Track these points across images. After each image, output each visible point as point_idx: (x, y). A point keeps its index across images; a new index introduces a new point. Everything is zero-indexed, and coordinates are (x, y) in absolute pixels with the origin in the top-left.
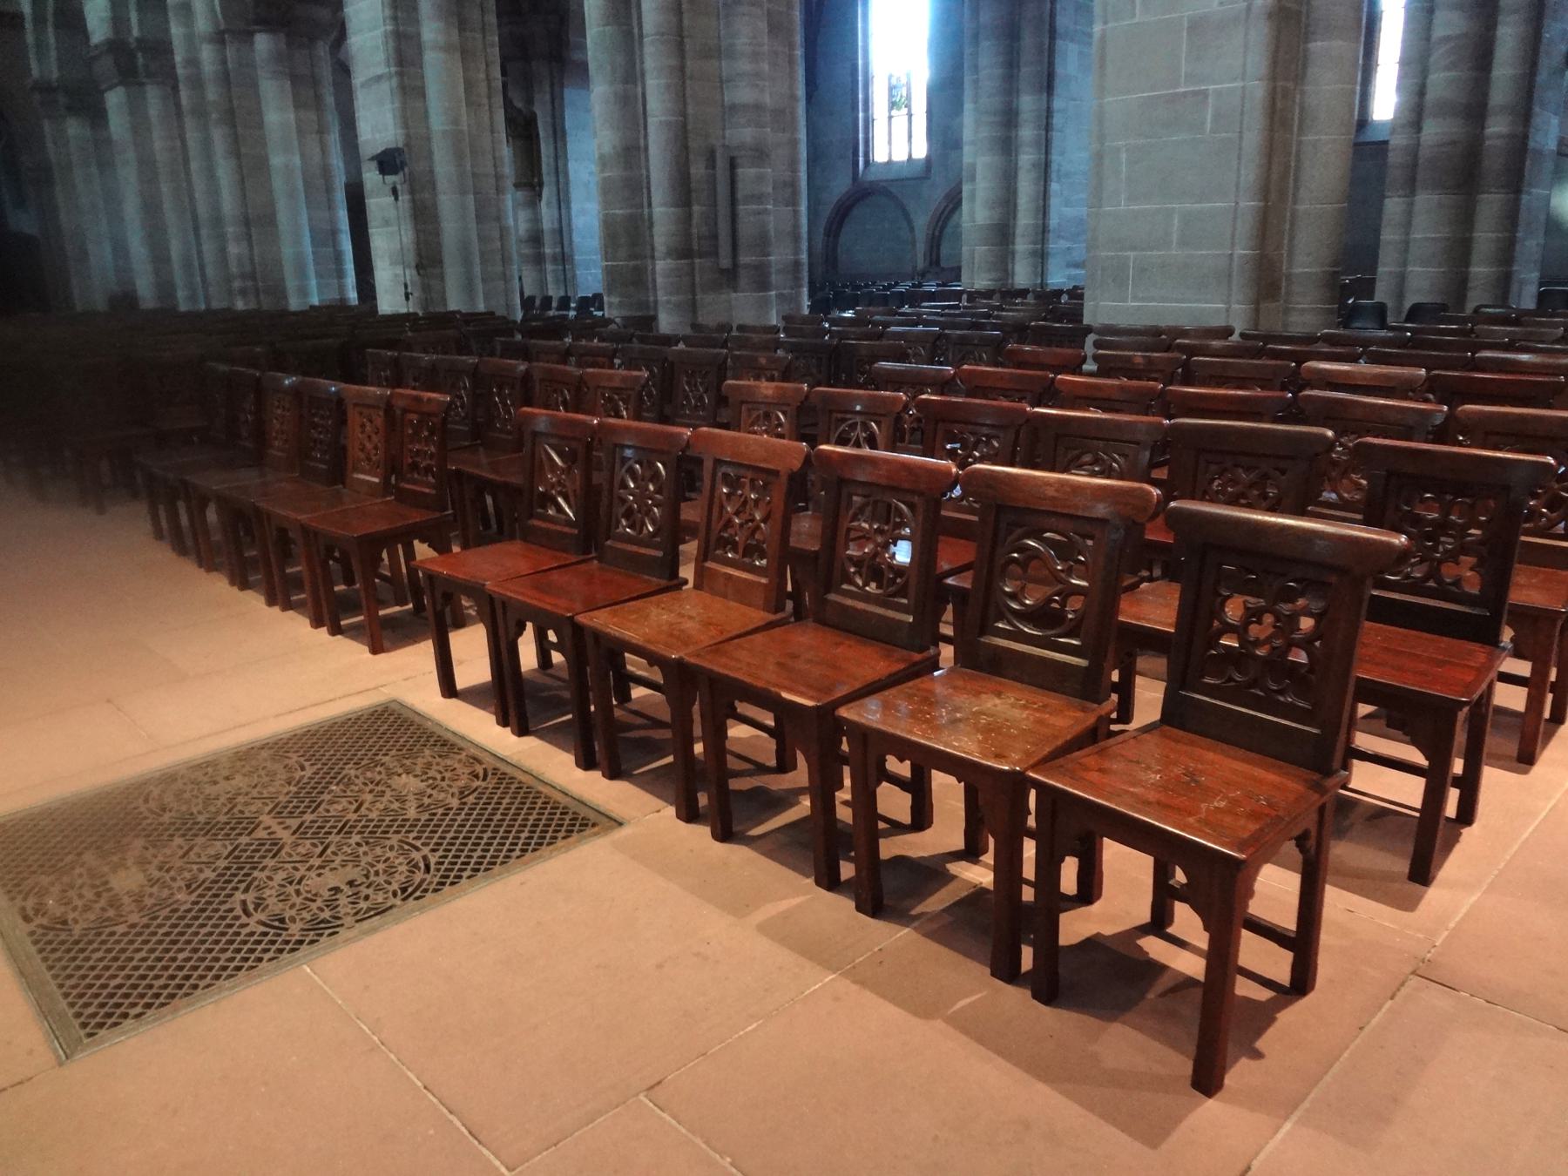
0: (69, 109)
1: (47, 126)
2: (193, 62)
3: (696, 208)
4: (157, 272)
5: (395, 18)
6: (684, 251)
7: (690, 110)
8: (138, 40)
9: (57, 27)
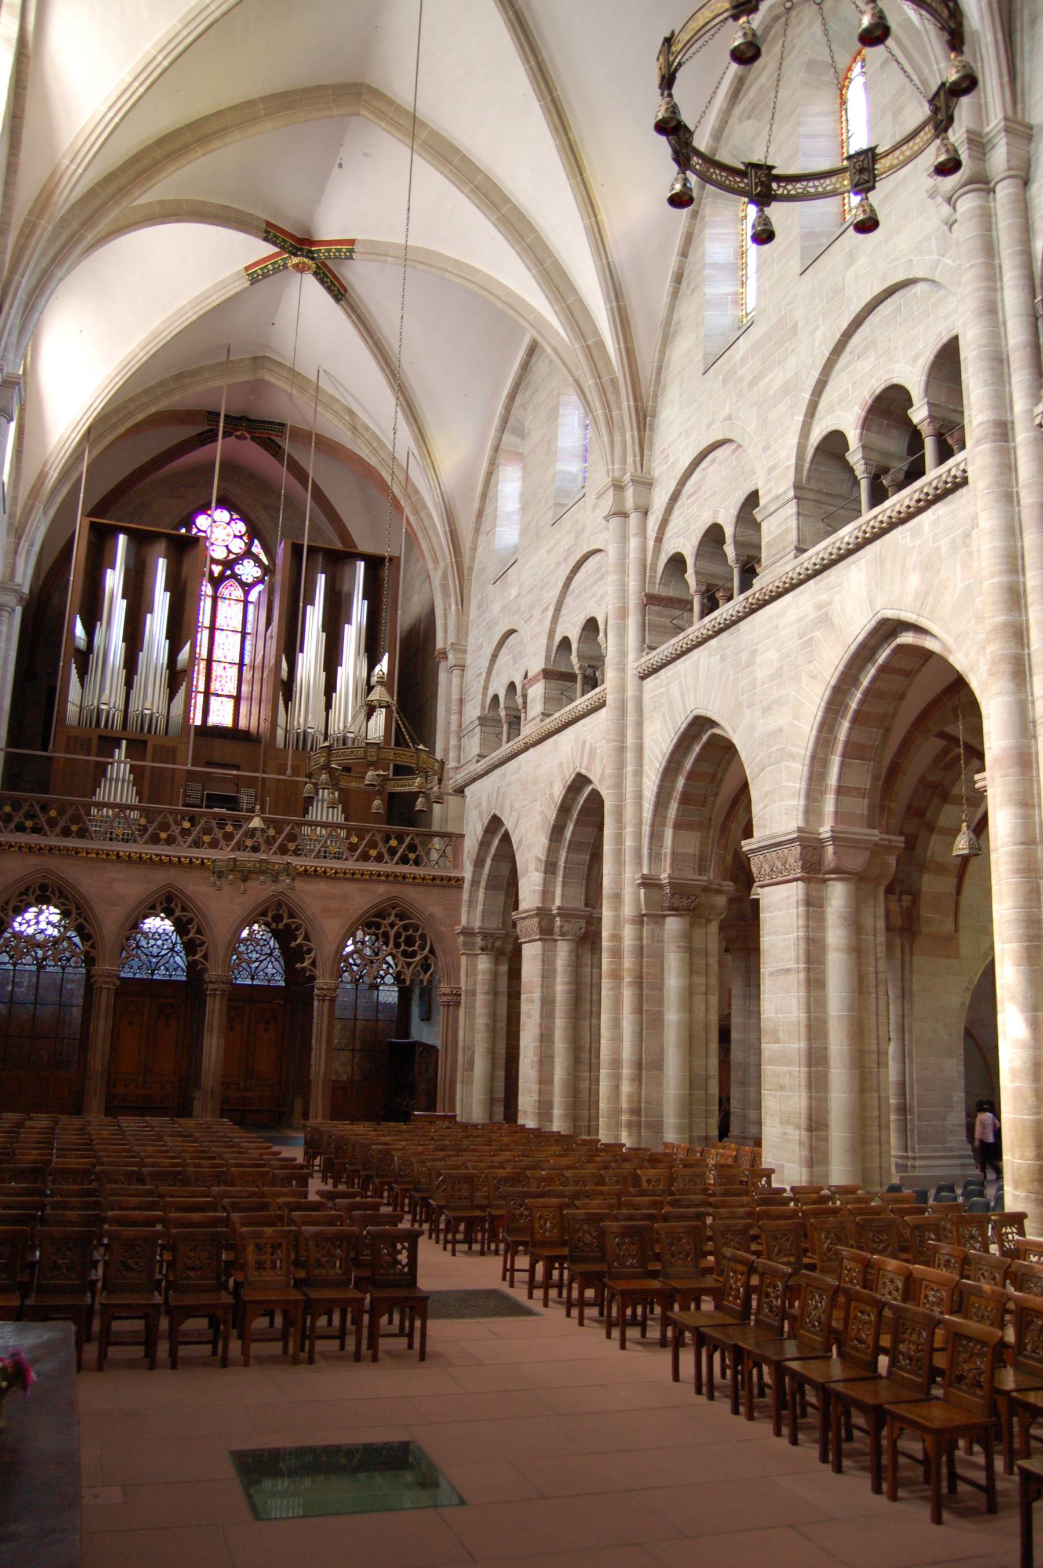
0: (483, 949)
1: (464, 959)
2: (617, 937)
5: (807, 927)
8: (559, 908)
9: (486, 889)
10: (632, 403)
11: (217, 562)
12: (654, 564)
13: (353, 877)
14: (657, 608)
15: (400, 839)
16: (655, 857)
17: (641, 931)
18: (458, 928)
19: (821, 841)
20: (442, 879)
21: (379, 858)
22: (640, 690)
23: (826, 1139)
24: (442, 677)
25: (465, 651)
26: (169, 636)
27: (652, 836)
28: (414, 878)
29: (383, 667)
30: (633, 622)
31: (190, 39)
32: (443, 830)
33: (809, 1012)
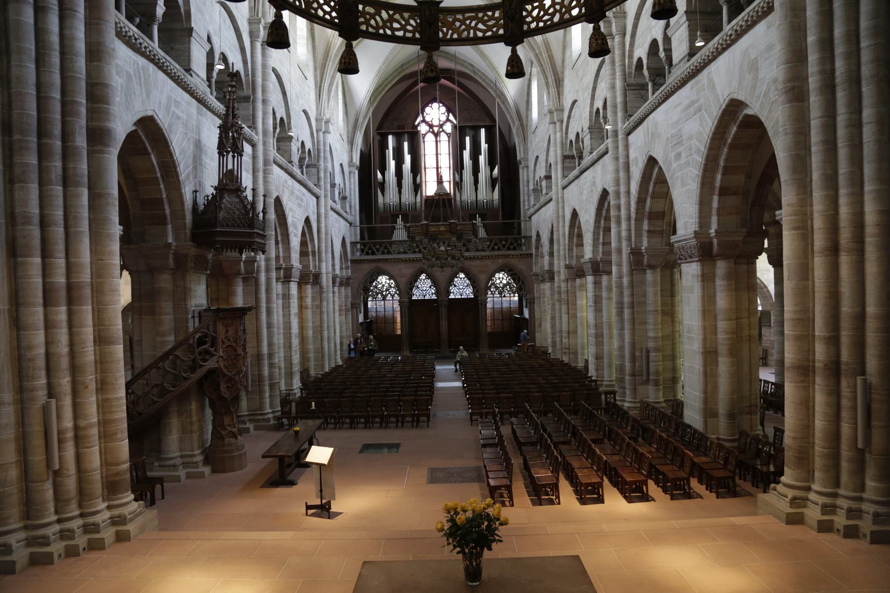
1: (535, 285)
2: (559, 287)
3: (637, 364)
4: (553, 338)
5: (595, 291)
6: (633, 375)
10: (553, 78)
11: (436, 126)
12: (566, 143)
13: (489, 257)
14: (568, 160)
15: (506, 241)
16: (571, 257)
20: (524, 255)
21: (499, 249)
22: (563, 193)
23: (603, 362)
24: (521, 171)
25: (528, 160)
26: (412, 172)
27: (569, 250)
28: (513, 256)
29: (496, 171)
30: (559, 166)
33: (596, 320)
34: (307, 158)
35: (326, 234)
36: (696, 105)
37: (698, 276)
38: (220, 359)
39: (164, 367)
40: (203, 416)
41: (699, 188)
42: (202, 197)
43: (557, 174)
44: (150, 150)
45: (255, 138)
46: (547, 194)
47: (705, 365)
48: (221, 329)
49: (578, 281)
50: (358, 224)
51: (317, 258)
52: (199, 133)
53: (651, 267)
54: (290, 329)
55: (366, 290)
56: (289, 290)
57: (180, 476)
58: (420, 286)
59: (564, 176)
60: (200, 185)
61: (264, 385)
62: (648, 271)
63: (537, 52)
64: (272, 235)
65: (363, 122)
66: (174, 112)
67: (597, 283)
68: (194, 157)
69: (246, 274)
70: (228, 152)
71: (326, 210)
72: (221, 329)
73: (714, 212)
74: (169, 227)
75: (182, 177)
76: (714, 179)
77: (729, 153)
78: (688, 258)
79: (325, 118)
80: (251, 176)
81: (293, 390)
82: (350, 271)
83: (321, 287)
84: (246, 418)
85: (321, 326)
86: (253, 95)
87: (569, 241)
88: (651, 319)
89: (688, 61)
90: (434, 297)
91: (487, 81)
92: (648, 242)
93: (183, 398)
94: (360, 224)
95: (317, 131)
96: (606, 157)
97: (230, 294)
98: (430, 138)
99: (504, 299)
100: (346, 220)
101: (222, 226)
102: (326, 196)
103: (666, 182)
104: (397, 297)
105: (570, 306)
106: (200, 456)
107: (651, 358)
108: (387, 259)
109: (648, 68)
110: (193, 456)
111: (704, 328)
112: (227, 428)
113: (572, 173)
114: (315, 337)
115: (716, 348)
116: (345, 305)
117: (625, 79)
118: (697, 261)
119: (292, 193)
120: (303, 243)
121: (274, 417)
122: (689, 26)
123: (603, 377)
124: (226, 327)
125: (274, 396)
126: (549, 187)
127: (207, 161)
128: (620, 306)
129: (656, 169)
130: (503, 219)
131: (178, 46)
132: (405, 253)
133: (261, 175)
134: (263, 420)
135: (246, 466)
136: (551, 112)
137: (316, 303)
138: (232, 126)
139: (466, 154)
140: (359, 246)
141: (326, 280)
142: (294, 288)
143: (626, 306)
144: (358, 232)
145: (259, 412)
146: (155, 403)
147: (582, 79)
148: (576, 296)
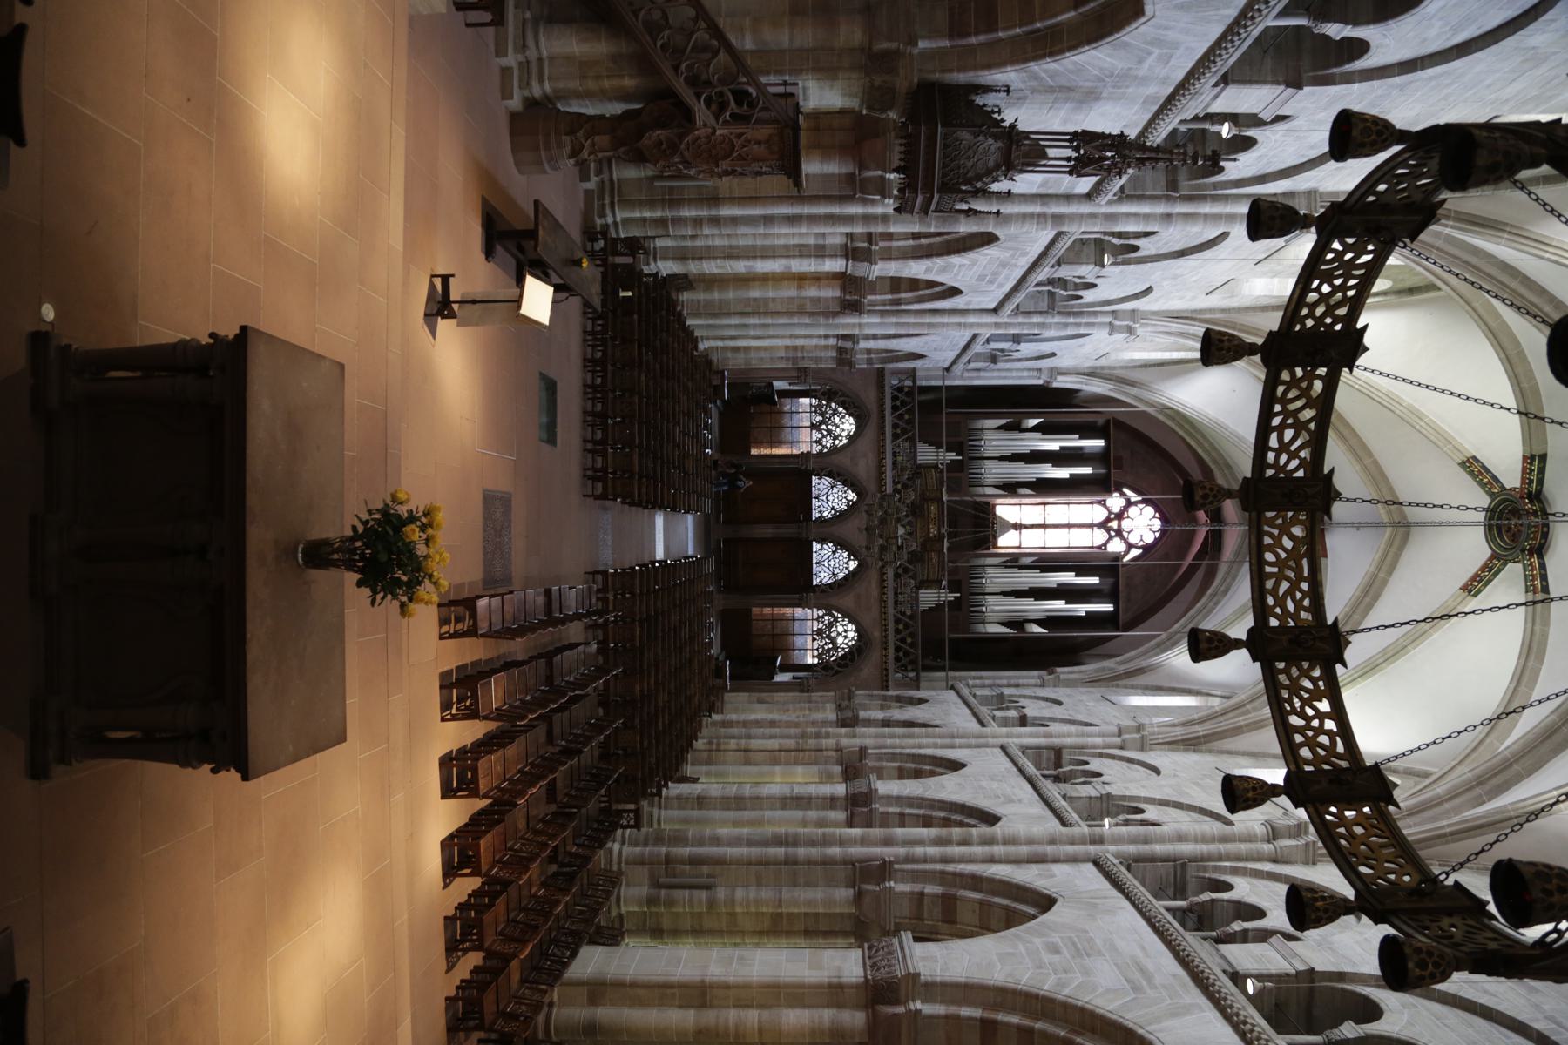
1: (832, 694)
2: (828, 736)
3: (688, 867)
4: (738, 722)
5: (818, 798)
6: (668, 860)
7: (734, 867)
11: (1119, 525)
12: (1084, 754)
14: (1053, 757)
15: (912, 645)
16: (880, 757)
17: (831, 750)
18: (853, 689)
19: (871, 805)
20: (887, 675)
21: (897, 631)
22: (993, 746)
23: (693, 809)
24: (1035, 673)
25: (1055, 686)
27: (893, 754)
28: (886, 656)
30: (1042, 741)
31: (1376, 398)
32: (922, 679)
33: (767, 798)
34: (1066, 293)
35: (930, 325)
36: (1144, 983)
37: (839, 977)
38: (710, 130)
39: (699, 30)
40: (610, 99)
41: (997, 983)
42: (998, 102)
43: (1028, 737)
44: (1082, 10)
45: (1103, 200)
46: (994, 718)
47: (683, 986)
48: (764, 132)
49: (838, 769)
50: (948, 383)
51: (888, 308)
52: (1112, 98)
53: (859, 897)
54: (763, 257)
55: (829, 395)
56: (831, 256)
57: (506, 55)
58: (835, 490)
59: (1024, 749)
60: (1019, 99)
61: (663, 209)
62: (850, 892)
63: (1248, 707)
64: (930, 227)
65: (1128, 395)
66: (1150, 54)
67: (831, 802)
68: (1069, 89)
69: (860, 180)
70: (1076, 149)
71: (972, 325)
72: (764, 132)
73: (953, 1010)
74: (945, 43)
75: (1034, 66)
76: (1012, 1010)
77: (1058, 1038)
78: (871, 962)
79: (1137, 325)
80: (1034, 191)
81: (655, 261)
82: (865, 366)
83: (835, 314)
84: (606, 176)
85: (766, 314)
86: (1179, 197)
87: (908, 755)
88: (766, 894)
89: (1224, 972)
90: (815, 515)
91: (1198, 617)
92: (903, 893)
93: (643, 63)
94: (947, 387)
95: (1113, 311)
96: (1056, 823)
97: (826, 151)
98: (1099, 514)
99: (809, 639)
100: (954, 362)
101: (946, 137)
102: (997, 325)
103: (1008, 928)
104: (816, 449)
105: (793, 753)
106: (541, 92)
107: (696, 893)
108: (883, 433)
109: (1213, 901)
110: (541, 80)
111: (746, 986)
112: (589, 141)
113: (1029, 763)
114: (748, 301)
115: (711, 1007)
116: (803, 358)
117: (1194, 859)
118: (866, 977)
119: (1004, 265)
120: (914, 284)
121: (607, 225)
122: (1287, 975)
123: (666, 808)
124: (767, 141)
125: (644, 226)
126: (1005, 722)
127: (1063, 113)
128: (790, 840)
129: (1032, 911)
130: (950, 640)
131: (1269, 63)
132: (894, 464)
133: (1037, 208)
134: (603, 205)
135: (521, 172)
136: (1140, 728)
137: (808, 304)
138: (1124, 157)
139: (1068, 578)
140: (908, 383)
141: (848, 323)
142: (835, 265)
143: (791, 850)
144: (933, 383)
145: (616, 199)
146: (636, 13)
147: (1197, 784)
148: (811, 764)
